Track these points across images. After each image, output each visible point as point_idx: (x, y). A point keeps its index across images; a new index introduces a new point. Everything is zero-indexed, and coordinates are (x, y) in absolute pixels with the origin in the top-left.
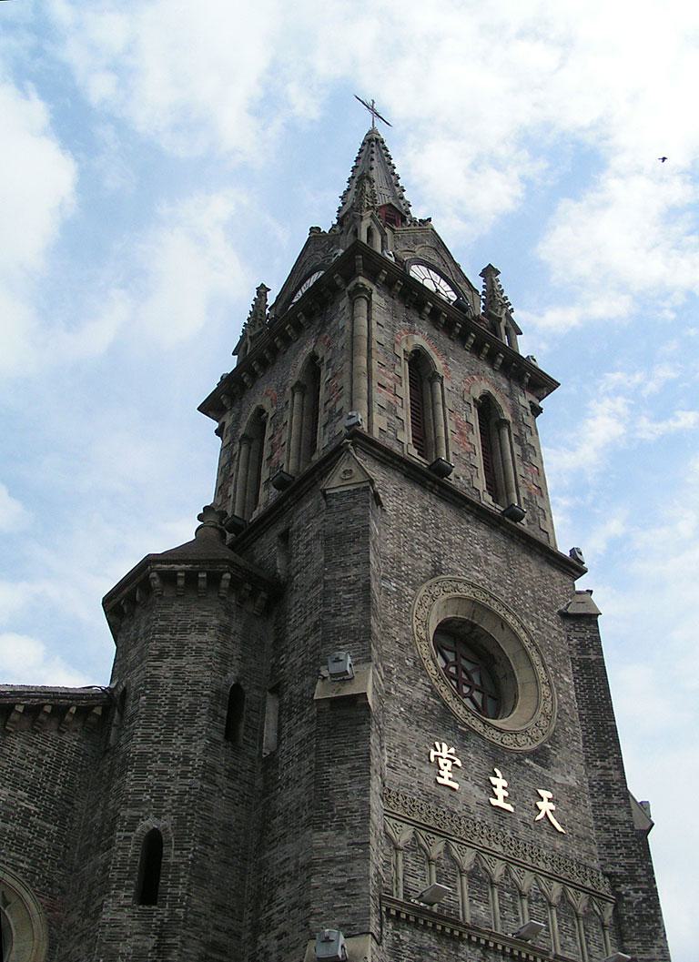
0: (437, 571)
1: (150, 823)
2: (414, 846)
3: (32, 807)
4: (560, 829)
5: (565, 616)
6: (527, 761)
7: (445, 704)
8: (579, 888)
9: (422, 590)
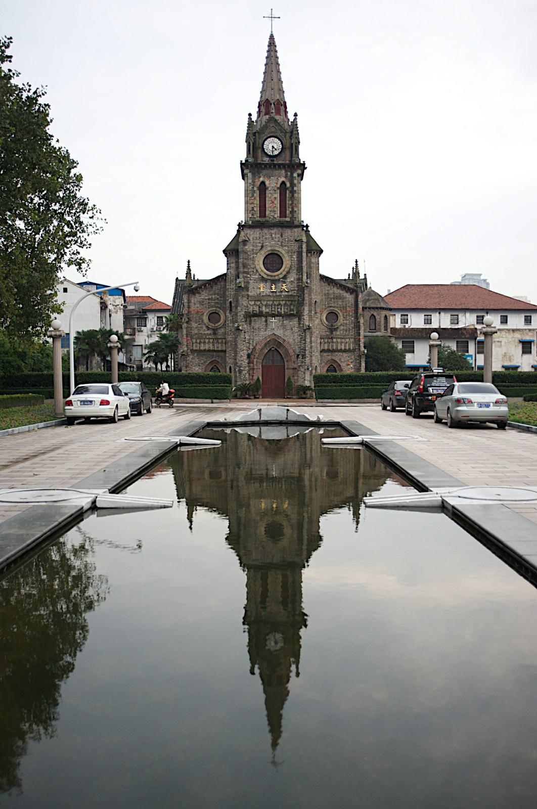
0: (262, 247)
1: (230, 300)
2: (255, 304)
4: (287, 290)
5: (296, 241)
6: (281, 280)
7: (262, 277)
8: (289, 301)
9: (258, 254)
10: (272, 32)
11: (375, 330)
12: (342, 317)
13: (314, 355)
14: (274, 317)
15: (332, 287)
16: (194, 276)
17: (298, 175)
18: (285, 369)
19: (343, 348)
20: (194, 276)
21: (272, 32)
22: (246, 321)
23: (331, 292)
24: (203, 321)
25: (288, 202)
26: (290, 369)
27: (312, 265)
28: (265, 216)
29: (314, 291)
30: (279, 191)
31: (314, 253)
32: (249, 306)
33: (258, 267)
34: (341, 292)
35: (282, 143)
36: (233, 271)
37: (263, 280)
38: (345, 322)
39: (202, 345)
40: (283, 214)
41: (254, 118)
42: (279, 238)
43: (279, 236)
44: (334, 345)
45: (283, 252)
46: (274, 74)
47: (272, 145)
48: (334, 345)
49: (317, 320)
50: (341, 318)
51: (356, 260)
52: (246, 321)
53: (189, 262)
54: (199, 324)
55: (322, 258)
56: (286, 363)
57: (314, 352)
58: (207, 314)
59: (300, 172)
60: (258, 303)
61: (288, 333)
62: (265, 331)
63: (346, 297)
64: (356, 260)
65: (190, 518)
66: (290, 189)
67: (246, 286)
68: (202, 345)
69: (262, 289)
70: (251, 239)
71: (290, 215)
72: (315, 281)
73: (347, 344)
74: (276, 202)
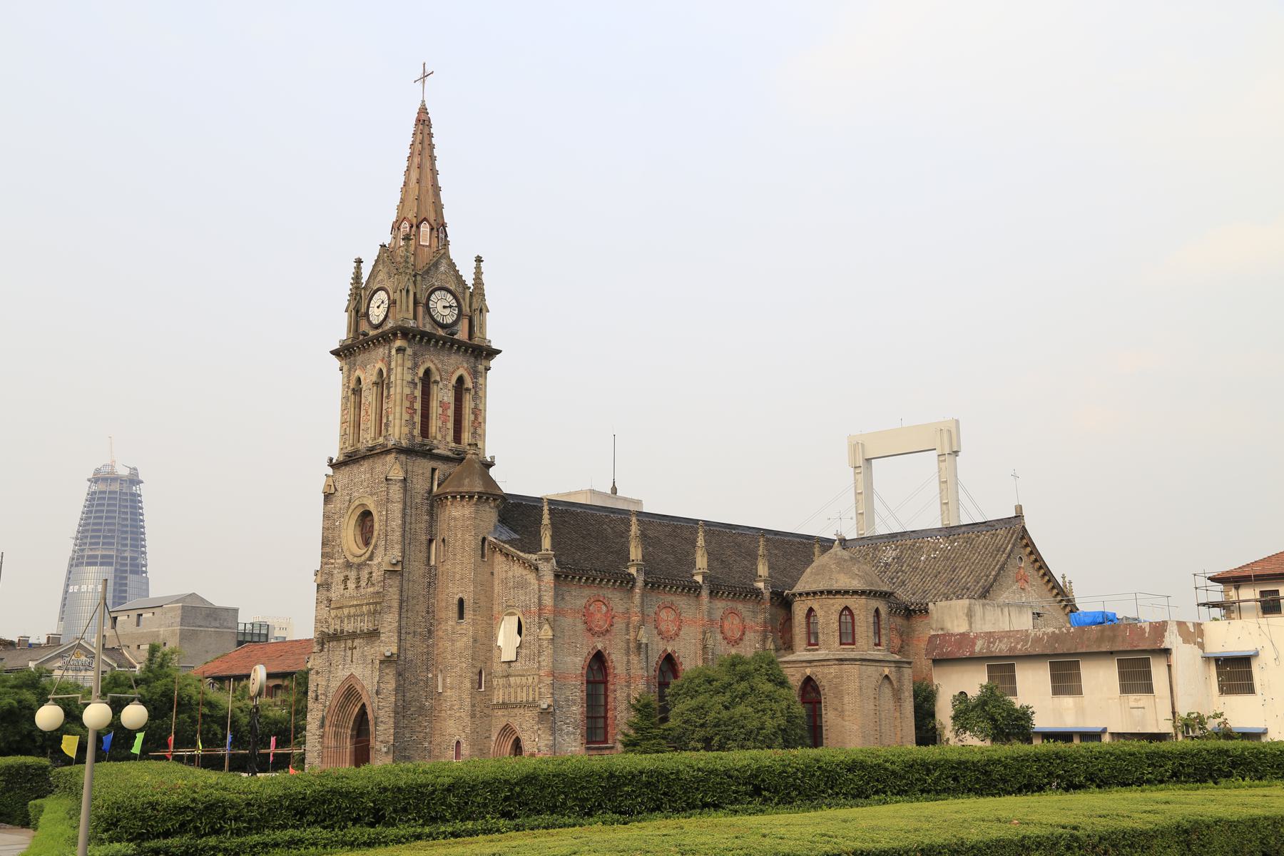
2: (336, 616)
10: (423, 101)
11: (817, 645)
13: (451, 716)
19: (524, 700)
21: (423, 101)
22: (321, 650)
23: (510, 574)
27: (452, 523)
29: (458, 577)
32: (330, 620)
33: (344, 541)
34: (525, 572)
43: (368, 475)
44: (512, 690)
48: (512, 690)
49: (465, 639)
52: (321, 650)
60: (339, 613)
61: (368, 672)
62: (343, 669)
63: (530, 583)
67: (326, 579)
70: (339, 490)
72: (459, 556)
73: (531, 689)
74: (370, 413)
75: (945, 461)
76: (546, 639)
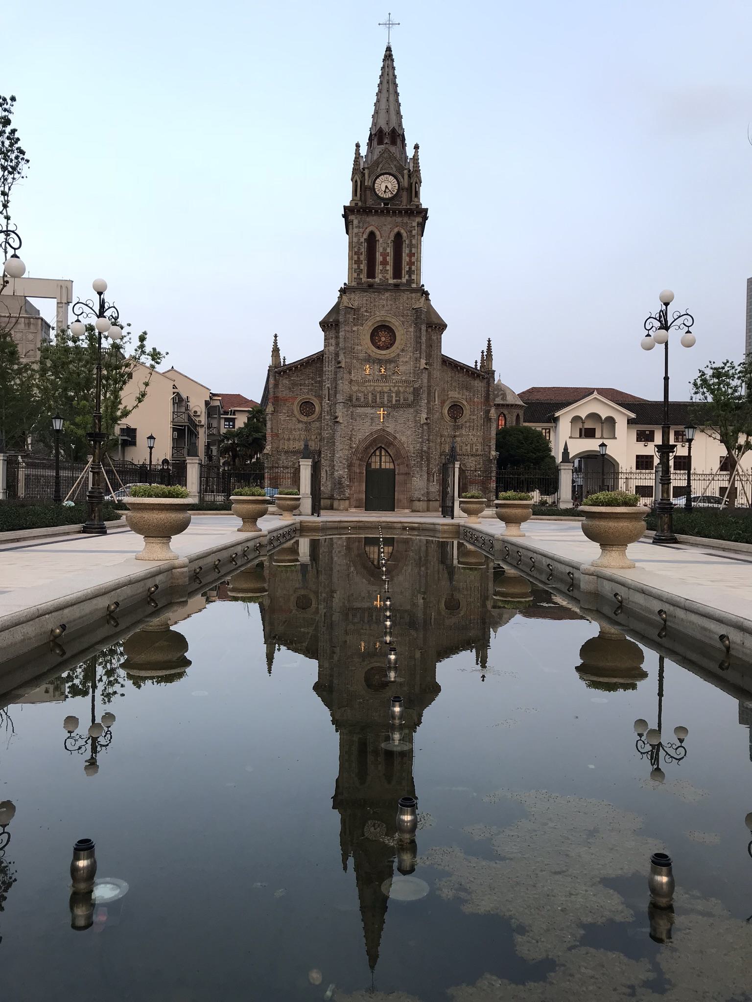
3: (313, 382)
10: (389, 43)
12: (468, 412)
14: (383, 407)
15: (457, 373)
16: (284, 359)
17: (418, 224)
18: (395, 475)
20: (284, 359)
21: (389, 43)
24: (293, 413)
25: (405, 258)
26: (402, 474)
28: (374, 277)
30: (392, 244)
31: (436, 327)
35: (398, 183)
36: (332, 348)
37: (369, 360)
38: (472, 417)
39: (291, 442)
40: (397, 274)
41: (363, 151)
42: (391, 305)
45: (397, 324)
46: (392, 98)
47: (386, 185)
50: (467, 412)
51: (489, 339)
53: (276, 336)
54: (288, 416)
55: (445, 336)
56: (396, 467)
57: (432, 454)
58: (298, 403)
59: (420, 219)
64: (489, 339)
65: (270, 658)
66: (407, 242)
68: (291, 442)
69: (368, 371)
71: (407, 277)
72: (435, 364)
75: (62, 307)
76: (494, 419)
